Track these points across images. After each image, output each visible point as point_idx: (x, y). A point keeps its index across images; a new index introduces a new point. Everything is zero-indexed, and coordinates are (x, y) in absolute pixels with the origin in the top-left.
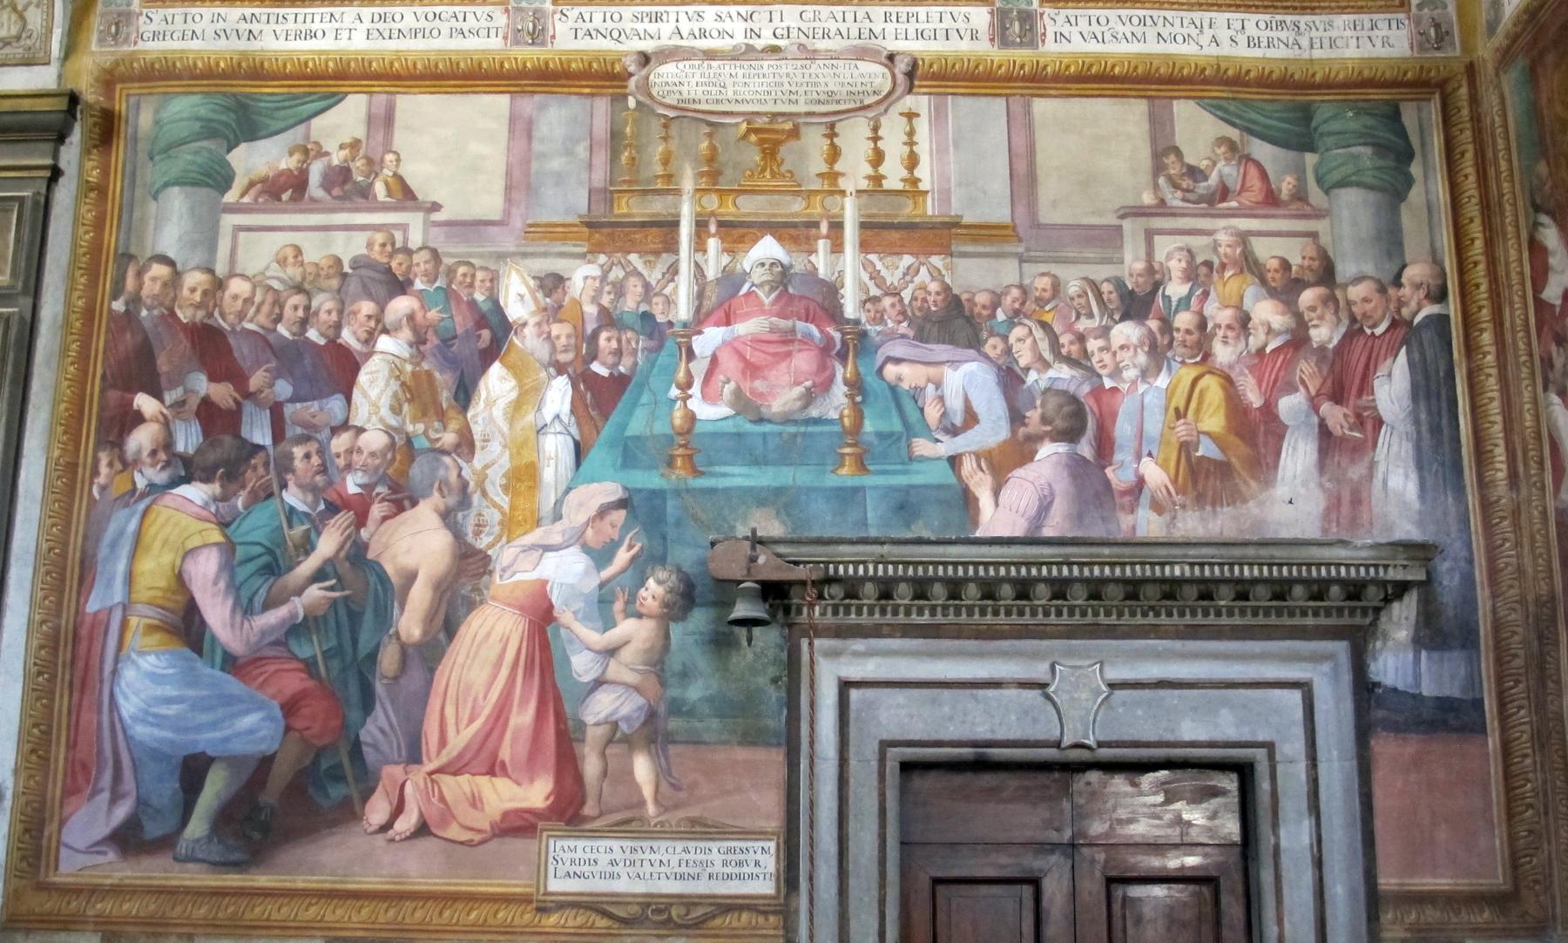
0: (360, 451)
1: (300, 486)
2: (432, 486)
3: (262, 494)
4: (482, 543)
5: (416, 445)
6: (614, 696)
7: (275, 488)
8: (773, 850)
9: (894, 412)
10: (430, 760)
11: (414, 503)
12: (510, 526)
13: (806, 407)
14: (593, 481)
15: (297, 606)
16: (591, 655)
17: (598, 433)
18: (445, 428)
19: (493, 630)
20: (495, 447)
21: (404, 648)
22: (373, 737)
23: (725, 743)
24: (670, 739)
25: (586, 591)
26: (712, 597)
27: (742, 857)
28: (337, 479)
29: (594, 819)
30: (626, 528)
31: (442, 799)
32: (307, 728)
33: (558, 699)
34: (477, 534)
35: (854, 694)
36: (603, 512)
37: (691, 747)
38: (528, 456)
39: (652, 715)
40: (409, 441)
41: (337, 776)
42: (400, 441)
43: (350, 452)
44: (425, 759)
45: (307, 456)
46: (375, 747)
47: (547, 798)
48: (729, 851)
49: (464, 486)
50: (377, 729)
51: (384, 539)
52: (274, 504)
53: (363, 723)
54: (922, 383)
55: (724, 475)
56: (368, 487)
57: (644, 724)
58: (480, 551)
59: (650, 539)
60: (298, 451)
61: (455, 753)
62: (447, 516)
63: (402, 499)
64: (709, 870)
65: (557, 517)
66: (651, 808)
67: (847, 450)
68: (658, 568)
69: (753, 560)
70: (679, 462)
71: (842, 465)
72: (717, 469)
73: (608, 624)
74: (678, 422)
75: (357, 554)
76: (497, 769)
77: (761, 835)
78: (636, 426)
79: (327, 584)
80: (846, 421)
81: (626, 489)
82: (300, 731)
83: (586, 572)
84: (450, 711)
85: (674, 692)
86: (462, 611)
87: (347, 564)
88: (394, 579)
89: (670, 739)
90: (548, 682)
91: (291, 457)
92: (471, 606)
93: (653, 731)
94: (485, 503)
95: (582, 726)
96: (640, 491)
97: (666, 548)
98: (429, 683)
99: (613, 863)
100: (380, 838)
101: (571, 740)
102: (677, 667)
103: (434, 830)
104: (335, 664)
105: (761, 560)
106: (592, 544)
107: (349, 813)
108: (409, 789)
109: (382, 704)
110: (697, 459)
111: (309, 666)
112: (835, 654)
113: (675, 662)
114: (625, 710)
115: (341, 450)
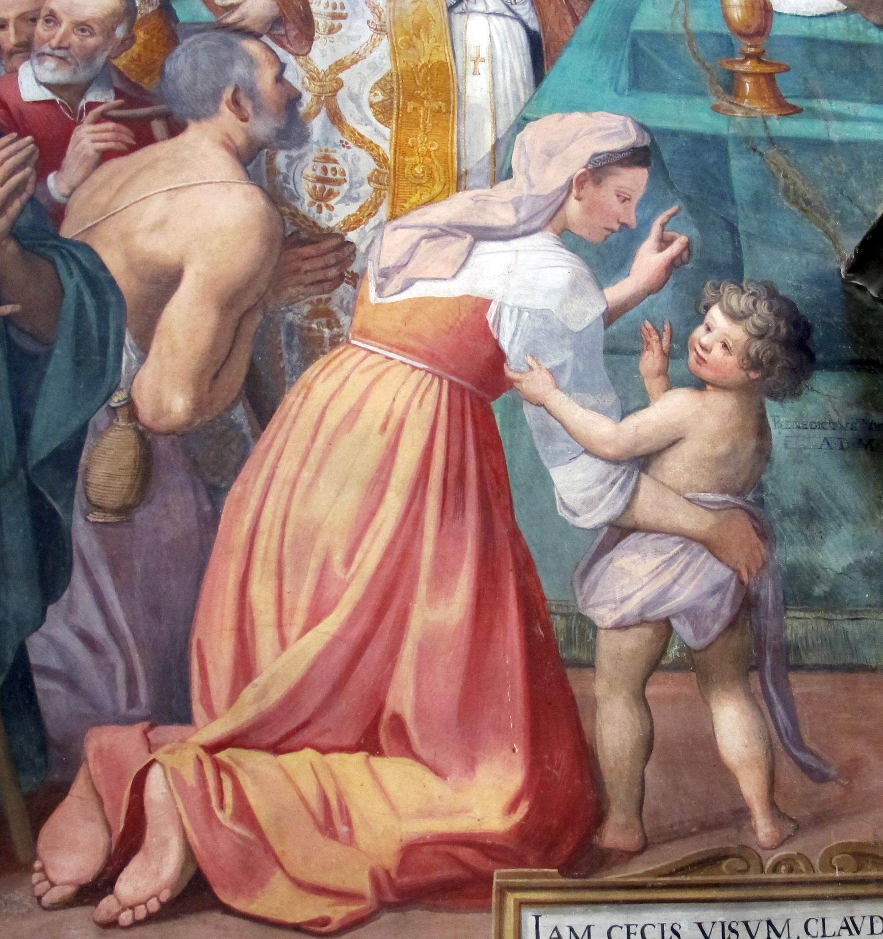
0: (52, 18)
2: (216, 96)
4: (335, 215)
6: (654, 562)
10: (212, 715)
11: (175, 129)
12: (396, 186)
14: (571, 107)
16: (598, 467)
17: (576, 21)
20: (358, 31)
21: (146, 440)
22: (63, 652)
24: (791, 659)
25: (576, 327)
26: (847, 351)
30: (650, 203)
31: (244, 812)
33: (525, 567)
34: (322, 198)
36: (599, 169)
37: (839, 677)
38: (428, 51)
44: (197, 708)
46: (70, 681)
47: (513, 807)
49: (292, 99)
50: (75, 635)
51: (102, 198)
53: (41, 618)
55: (841, 117)
56: (70, 91)
57: (732, 624)
58: (330, 234)
59: (701, 228)
61: (275, 695)
62: (251, 159)
63: (147, 118)
65: (501, 172)
68: (728, 288)
72: (825, 105)
73: (631, 401)
76: (383, 737)
81: (642, 127)
83: (573, 285)
84: (261, 594)
85: (791, 553)
86: (290, 359)
87: (12, 247)
88: (125, 282)
89: (791, 659)
90: (501, 530)
92: (311, 349)
94: (337, 137)
95: (587, 629)
96: (674, 134)
97: (738, 249)
98: (210, 523)
101: (562, 665)
102: (792, 498)
103: (225, 897)
106: (584, 233)
108: (156, 786)
109: (88, 573)
110: (784, 82)
113: (788, 482)
114: (685, 594)
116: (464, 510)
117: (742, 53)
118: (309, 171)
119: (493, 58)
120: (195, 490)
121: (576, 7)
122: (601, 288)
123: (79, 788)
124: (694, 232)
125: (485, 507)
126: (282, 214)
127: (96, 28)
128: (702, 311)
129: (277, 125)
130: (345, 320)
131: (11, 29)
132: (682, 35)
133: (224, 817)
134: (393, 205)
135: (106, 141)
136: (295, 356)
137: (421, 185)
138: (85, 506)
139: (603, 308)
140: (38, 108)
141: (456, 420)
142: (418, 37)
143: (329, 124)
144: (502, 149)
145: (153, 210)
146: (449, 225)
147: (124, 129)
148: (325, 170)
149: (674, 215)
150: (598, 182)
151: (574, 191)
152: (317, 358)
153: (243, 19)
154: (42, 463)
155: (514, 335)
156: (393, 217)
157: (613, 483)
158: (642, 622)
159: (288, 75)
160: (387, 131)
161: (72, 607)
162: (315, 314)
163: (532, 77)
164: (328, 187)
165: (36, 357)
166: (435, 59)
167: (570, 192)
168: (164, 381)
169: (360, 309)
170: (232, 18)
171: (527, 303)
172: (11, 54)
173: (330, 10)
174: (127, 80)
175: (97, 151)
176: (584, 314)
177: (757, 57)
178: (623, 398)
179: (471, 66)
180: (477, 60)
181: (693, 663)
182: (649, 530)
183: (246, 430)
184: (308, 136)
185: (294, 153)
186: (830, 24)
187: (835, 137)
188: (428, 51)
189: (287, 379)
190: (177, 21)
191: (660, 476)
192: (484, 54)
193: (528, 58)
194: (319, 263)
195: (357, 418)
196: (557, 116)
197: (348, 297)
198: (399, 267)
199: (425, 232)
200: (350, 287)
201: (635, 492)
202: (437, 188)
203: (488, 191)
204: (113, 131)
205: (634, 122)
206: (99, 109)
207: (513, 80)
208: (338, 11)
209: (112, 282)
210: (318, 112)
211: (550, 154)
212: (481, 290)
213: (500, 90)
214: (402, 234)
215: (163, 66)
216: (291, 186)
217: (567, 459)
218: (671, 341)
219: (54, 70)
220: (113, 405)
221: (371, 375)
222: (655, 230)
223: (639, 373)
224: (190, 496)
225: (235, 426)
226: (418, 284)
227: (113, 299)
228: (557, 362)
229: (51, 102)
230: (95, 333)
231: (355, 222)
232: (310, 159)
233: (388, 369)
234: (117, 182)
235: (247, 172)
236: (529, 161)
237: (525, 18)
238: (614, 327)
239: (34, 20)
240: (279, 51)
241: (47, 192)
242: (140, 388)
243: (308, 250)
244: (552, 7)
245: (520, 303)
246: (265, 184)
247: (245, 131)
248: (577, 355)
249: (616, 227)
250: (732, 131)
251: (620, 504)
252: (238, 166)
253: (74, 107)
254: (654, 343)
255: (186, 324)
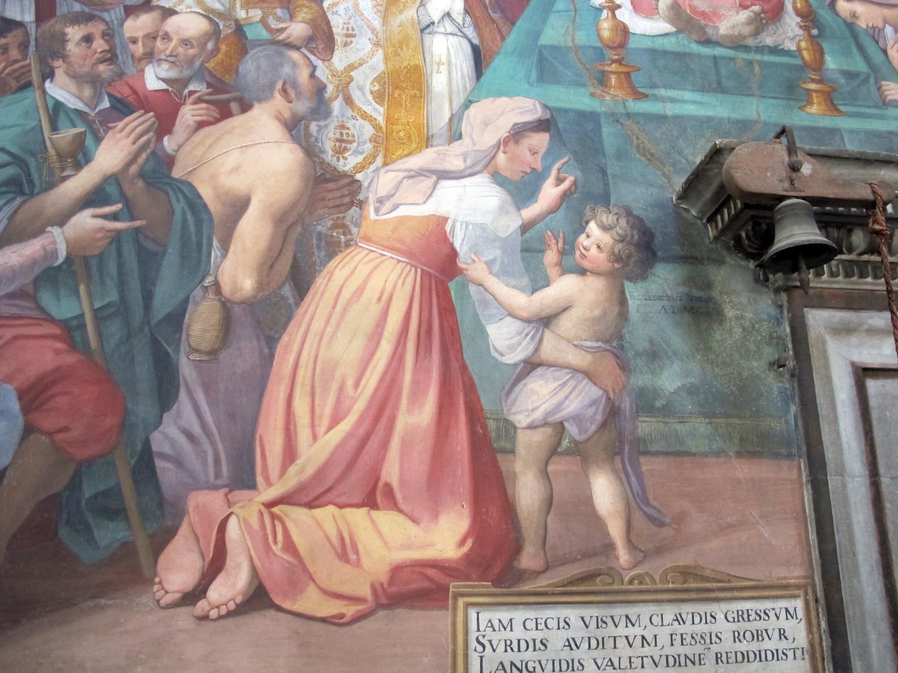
0: (167, 37)
1: (75, 77)
2: (272, 86)
3: (14, 84)
4: (349, 163)
5: (251, 33)
6: (553, 385)
7: (35, 77)
8: (801, 613)
9: (855, 51)
10: (269, 484)
11: (246, 107)
12: (388, 145)
13: (756, 33)
14: (499, 94)
15: (57, 241)
16: (518, 325)
17: (503, 38)
18: (292, 17)
19: (365, 285)
20: (363, 45)
21: (226, 306)
22: (173, 443)
23: (718, 453)
25: (503, 234)
26: (677, 250)
27: (760, 625)
28: (131, 70)
29: (536, 574)
30: (551, 155)
31: (290, 546)
32: (65, 429)
33: (470, 389)
34: (340, 152)
35: (873, 386)
36: (518, 133)
38: (408, 58)
39: (613, 413)
40: (239, 29)
41: (110, 508)
42: (226, 29)
43: (152, 37)
44: (260, 480)
45: (88, 39)
46: (178, 462)
47: (462, 542)
48: (742, 616)
49: (320, 89)
50: (181, 432)
51: (199, 152)
52: (32, 97)
54: (880, 24)
55: (673, 100)
56: (178, 83)
57: (603, 425)
58: (345, 175)
59: (583, 171)
60: (74, 33)
61: (310, 471)
62: (294, 127)
64: (715, 648)
65: (455, 135)
66: (623, 556)
67: (813, 86)
68: (600, 210)
69: (795, 168)
70: (613, 80)
71: (810, 103)
72: (663, 92)
73: (538, 282)
74: (606, 34)
75: (155, 168)
77: (781, 590)
78: (554, 33)
79: (107, 210)
80: (805, 54)
81: (545, 107)
82: (49, 434)
83: (501, 208)
84: (301, 406)
85: (640, 380)
87: (140, 183)
90: (455, 365)
91: (63, 39)
92: (333, 249)
93: (616, 436)
94: (349, 113)
95: (509, 429)
96: (566, 111)
97: (607, 185)
98: (268, 360)
99: (572, 644)
100: (183, 618)
101: (494, 451)
102: (641, 344)
103: (277, 601)
104: (114, 330)
105: (806, 169)
107: (130, 571)
108: (233, 529)
109: (190, 393)
110: (636, 78)
111: (70, 332)
112: (844, 331)
113: (639, 334)
114: (573, 406)
115: (140, 34)
116: (431, 352)
117: (610, 59)
118: (331, 135)
119: (449, 62)
120: (258, 339)
121: (503, 30)
122: (519, 209)
123: (184, 530)
124: (579, 174)
125: (444, 349)
126: (314, 162)
127: (195, 43)
128: (584, 224)
129: (310, 105)
130: (354, 230)
131: (140, 44)
132: (571, 48)
133: (277, 549)
134: (385, 157)
135: (201, 115)
136: (323, 254)
137: (403, 144)
138: (187, 349)
139: (520, 223)
140: (157, 94)
141: (426, 294)
142: (402, 49)
143: (344, 105)
144: (455, 121)
145: (231, 160)
146: (421, 170)
147: (212, 107)
148: (342, 134)
149: (566, 163)
150: (517, 142)
151: (502, 148)
152: (337, 255)
153: (289, 37)
154: (160, 322)
155: (463, 240)
156: (385, 164)
157: (527, 335)
158: (546, 424)
159: (318, 73)
160: (381, 109)
161: (179, 414)
162: (335, 227)
163: (474, 74)
164: (343, 145)
165: (156, 254)
166: (412, 63)
167: (499, 148)
168: (238, 269)
169: (364, 223)
170: (281, 38)
171: (472, 219)
172: (140, 60)
173: (345, 31)
174: (215, 76)
175: (195, 122)
176: (508, 226)
177: (619, 62)
178: (533, 281)
179: (435, 67)
180: (439, 63)
181: (578, 450)
182: (550, 365)
183: (291, 301)
184: (331, 113)
185: (322, 123)
186: (666, 41)
187: (669, 113)
188: (408, 58)
189: (317, 268)
190: (247, 38)
191: (557, 331)
192: (444, 60)
193: (472, 63)
194: (338, 194)
195: (363, 293)
196: (490, 100)
197: (356, 216)
198: (389, 197)
199: (406, 174)
200: (358, 209)
201: (541, 340)
202: (414, 146)
203: (446, 147)
204: (206, 109)
205: (541, 103)
206: (197, 95)
207: (463, 77)
208: (350, 32)
209: (205, 206)
210: (337, 97)
211: (486, 124)
212: (442, 211)
213: (454, 83)
214: (391, 175)
215: (238, 67)
216: (320, 144)
217: (497, 319)
218: (564, 243)
219: (167, 70)
220: (205, 285)
221: (372, 265)
222: (554, 172)
223: (543, 264)
224: (255, 343)
225: (284, 299)
226: (402, 207)
227: (205, 217)
228: (491, 257)
229: (166, 91)
230: (194, 238)
231: (361, 168)
232: (332, 127)
233: (382, 262)
234: (208, 142)
235: (292, 135)
236: (473, 128)
237: (470, 37)
238: (527, 235)
239: (155, 38)
240: (312, 58)
241: (163, 148)
242: (223, 273)
243: (331, 186)
244: (488, 29)
245: (466, 219)
246: (303, 143)
247: (291, 109)
248: (503, 253)
249: (529, 170)
250: (603, 109)
251: (531, 348)
252: (286, 131)
253: (181, 93)
254: (553, 245)
255: (253, 232)
